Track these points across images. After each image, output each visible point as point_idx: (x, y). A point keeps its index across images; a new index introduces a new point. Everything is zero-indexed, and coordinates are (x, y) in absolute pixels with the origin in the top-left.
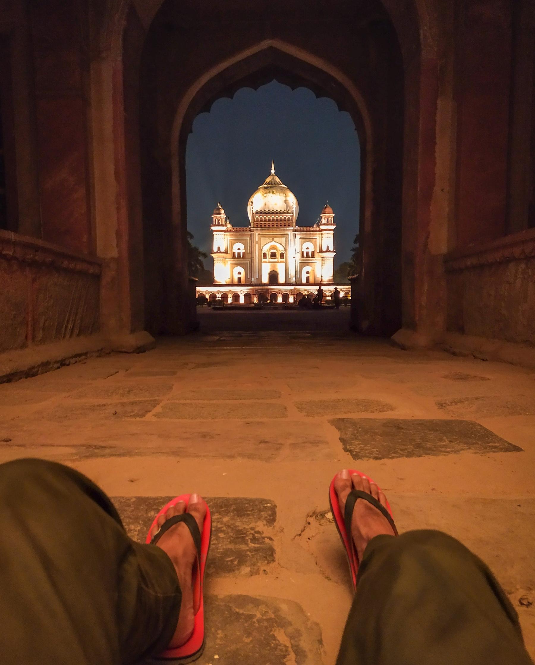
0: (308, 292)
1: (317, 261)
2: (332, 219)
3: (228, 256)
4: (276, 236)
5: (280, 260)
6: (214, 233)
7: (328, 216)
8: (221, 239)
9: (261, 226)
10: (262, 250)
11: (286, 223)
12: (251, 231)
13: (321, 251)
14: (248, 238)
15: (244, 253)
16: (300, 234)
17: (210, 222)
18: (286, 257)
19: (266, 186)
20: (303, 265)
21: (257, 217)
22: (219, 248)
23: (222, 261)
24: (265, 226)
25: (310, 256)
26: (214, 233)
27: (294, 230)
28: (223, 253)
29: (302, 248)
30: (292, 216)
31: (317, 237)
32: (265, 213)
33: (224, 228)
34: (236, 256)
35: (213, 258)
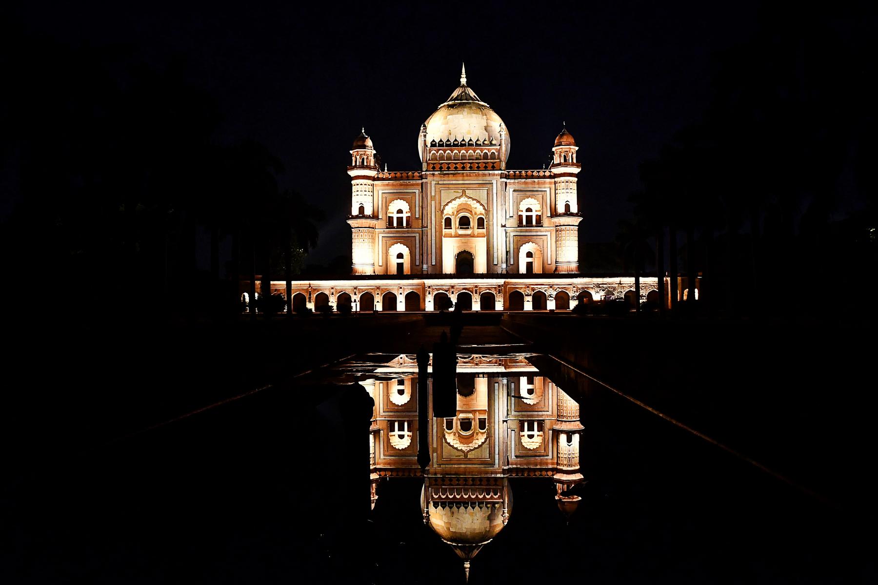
0: (533, 289)
1: (547, 230)
2: (574, 155)
3: (380, 224)
4: (469, 186)
5: (477, 231)
6: (353, 182)
7: (565, 150)
8: (367, 193)
9: (441, 168)
10: (442, 212)
11: (487, 164)
12: (421, 177)
13: (554, 214)
14: (417, 192)
17: (348, 163)
18: (488, 225)
19: (450, 103)
20: (521, 240)
22: (362, 209)
24: (448, 168)
25: (534, 223)
26: (353, 182)
28: (368, 217)
29: (518, 210)
30: (499, 151)
31: (548, 190)
32: (447, 145)
33: (372, 173)
34: (395, 224)
35: (350, 228)
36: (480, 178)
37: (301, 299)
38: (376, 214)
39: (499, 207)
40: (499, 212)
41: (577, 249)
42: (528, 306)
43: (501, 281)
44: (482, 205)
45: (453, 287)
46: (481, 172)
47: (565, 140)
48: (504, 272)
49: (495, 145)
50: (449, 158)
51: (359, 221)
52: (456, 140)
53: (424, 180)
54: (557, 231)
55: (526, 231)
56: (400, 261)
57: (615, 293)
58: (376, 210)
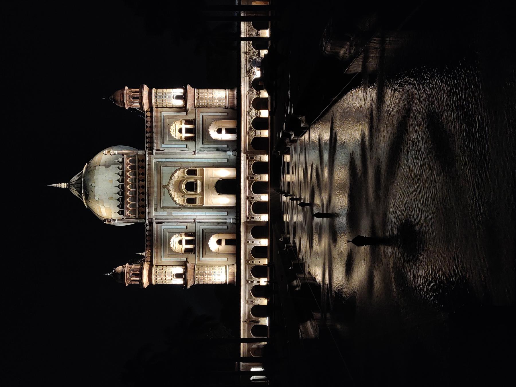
0: (250, 129)
1: (200, 116)
2: (133, 90)
3: (192, 260)
5: (198, 176)
6: (154, 283)
7: (128, 98)
10: (181, 206)
12: (151, 224)
15: (187, 235)
16: (157, 143)
18: (193, 166)
21: (128, 213)
22: (178, 276)
23: (198, 270)
26: (154, 283)
27: (151, 154)
29: (180, 140)
30: (128, 156)
31: (163, 114)
33: (146, 266)
35: (193, 286)
36: (152, 173)
37: (258, 330)
38: (183, 263)
39: (179, 156)
40: (182, 156)
41: (215, 90)
42: (265, 133)
43: (243, 156)
44: (176, 172)
45: (248, 198)
46: (147, 172)
47: (119, 98)
48: (235, 153)
49: (123, 159)
50: (134, 199)
51: (188, 277)
52: (118, 193)
53: (154, 221)
54: (199, 107)
55: (199, 133)
56: (223, 243)
57: (255, 57)
58: (178, 263)
